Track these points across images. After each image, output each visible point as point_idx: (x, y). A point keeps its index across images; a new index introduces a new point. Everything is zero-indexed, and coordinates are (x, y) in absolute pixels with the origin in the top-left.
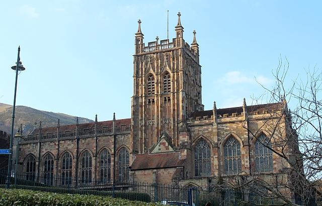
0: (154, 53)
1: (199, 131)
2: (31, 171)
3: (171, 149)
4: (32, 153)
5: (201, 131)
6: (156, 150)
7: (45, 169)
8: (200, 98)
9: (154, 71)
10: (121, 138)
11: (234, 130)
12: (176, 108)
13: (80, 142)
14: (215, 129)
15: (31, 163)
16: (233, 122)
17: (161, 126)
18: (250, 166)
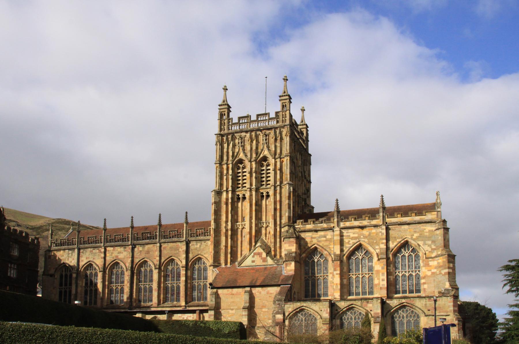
0: (247, 132)
1: (312, 238)
2: (66, 285)
3: (270, 261)
5: (315, 238)
6: (248, 262)
8: (309, 196)
9: (246, 156)
10: (193, 246)
11: (365, 237)
12: (278, 207)
13: (136, 249)
14: (337, 235)
15: (66, 275)
16: (362, 228)
17: (256, 231)
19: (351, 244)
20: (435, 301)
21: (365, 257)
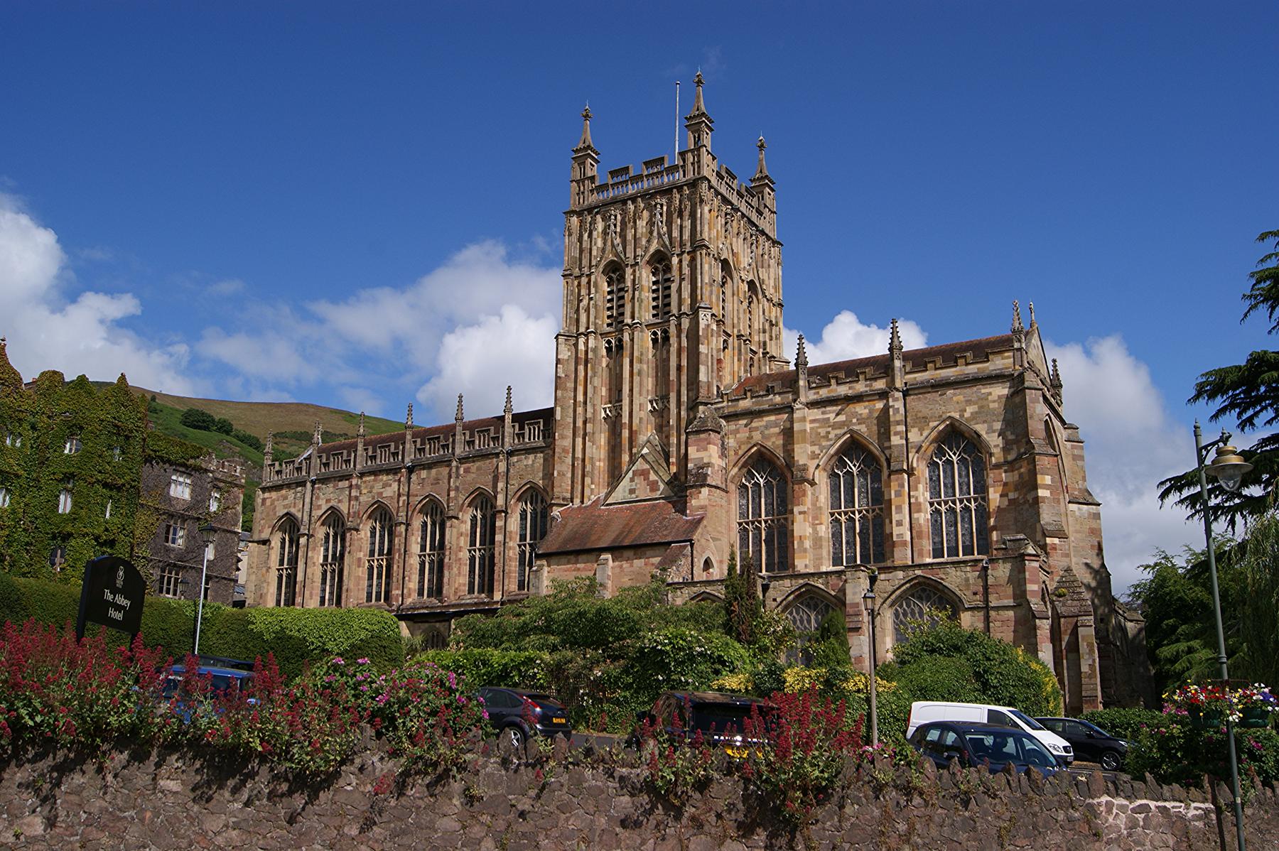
4: (293, 510)
5: (756, 429)
7: (326, 557)
13: (414, 477)
18: (912, 538)
19: (831, 440)
20: (985, 569)
21: (865, 468)
